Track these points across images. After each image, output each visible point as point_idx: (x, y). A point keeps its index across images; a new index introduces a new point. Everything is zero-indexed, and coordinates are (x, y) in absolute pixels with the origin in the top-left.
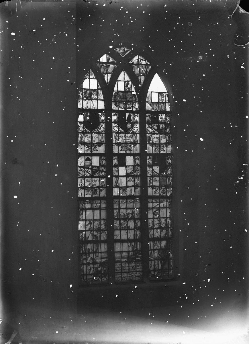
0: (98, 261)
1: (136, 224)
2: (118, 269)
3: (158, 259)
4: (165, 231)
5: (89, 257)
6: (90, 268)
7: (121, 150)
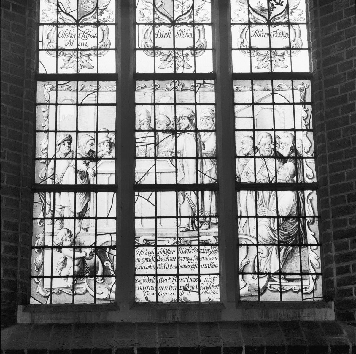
0: (87, 240)
1: (199, 144)
4: (290, 166)
6: (62, 260)
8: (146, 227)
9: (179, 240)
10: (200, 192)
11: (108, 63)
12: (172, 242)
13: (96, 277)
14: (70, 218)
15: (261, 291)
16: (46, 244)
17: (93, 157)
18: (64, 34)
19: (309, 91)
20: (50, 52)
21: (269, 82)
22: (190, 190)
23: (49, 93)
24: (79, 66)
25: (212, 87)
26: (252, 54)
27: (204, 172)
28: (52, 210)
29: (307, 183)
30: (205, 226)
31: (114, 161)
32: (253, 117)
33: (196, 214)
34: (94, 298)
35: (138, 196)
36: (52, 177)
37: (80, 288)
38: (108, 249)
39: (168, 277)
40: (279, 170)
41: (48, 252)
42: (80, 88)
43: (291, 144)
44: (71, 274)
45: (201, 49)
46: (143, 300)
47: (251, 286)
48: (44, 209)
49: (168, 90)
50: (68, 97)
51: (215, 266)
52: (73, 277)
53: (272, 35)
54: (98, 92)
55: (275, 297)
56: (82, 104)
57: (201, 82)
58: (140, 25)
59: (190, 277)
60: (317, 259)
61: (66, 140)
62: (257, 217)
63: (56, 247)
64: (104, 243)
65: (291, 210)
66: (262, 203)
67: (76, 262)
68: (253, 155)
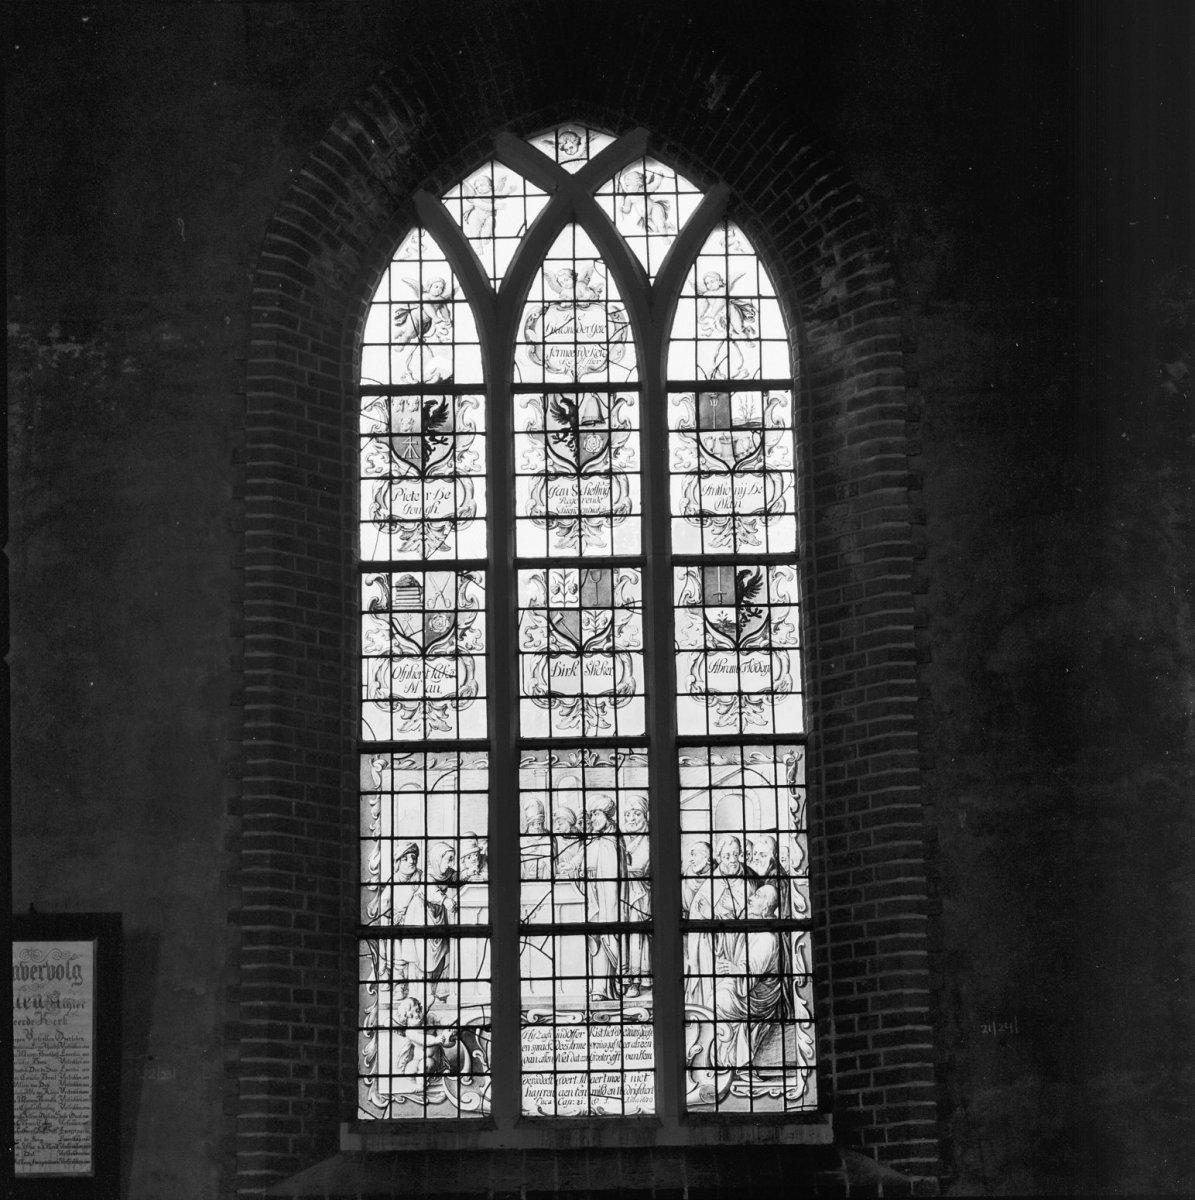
0: (446, 1016)
1: (623, 857)
2: (540, 1054)
4: (768, 892)
6: (407, 1048)
7: (561, 546)
9: (591, 1015)
10: (623, 936)
11: (475, 723)
12: (579, 1018)
14: (417, 981)
15: (720, 1097)
16: (380, 1024)
17: (452, 881)
18: (403, 672)
19: (802, 764)
20: (380, 703)
21: (737, 749)
22: (609, 934)
24: (428, 728)
25: (644, 760)
27: (631, 904)
28: (389, 967)
29: (796, 921)
30: (632, 992)
31: (487, 885)
32: (711, 810)
33: (618, 972)
34: (456, 1110)
35: (526, 943)
36: (387, 914)
37: (435, 1093)
38: (478, 1031)
39: (573, 1075)
41: (384, 1036)
42: (430, 764)
43: (770, 855)
44: (421, 1071)
45: (626, 696)
46: (534, 1112)
47: (705, 1088)
48: (377, 967)
49: (573, 766)
51: (648, 1056)
52: (424, 1075)
53: (742, 669)
54: (458, 770)
55: (741, 1106)
56: (432, 792)
57: (626, 751)
58: (525, 656)
59: (608, 1074)
60: (810, 1045)
61: (408, 853)
62: (714, 976)
63: (397, 1029)
64: (472, 1021)
65: (770, 964)
66: (723, 952)
68: (708, 874)
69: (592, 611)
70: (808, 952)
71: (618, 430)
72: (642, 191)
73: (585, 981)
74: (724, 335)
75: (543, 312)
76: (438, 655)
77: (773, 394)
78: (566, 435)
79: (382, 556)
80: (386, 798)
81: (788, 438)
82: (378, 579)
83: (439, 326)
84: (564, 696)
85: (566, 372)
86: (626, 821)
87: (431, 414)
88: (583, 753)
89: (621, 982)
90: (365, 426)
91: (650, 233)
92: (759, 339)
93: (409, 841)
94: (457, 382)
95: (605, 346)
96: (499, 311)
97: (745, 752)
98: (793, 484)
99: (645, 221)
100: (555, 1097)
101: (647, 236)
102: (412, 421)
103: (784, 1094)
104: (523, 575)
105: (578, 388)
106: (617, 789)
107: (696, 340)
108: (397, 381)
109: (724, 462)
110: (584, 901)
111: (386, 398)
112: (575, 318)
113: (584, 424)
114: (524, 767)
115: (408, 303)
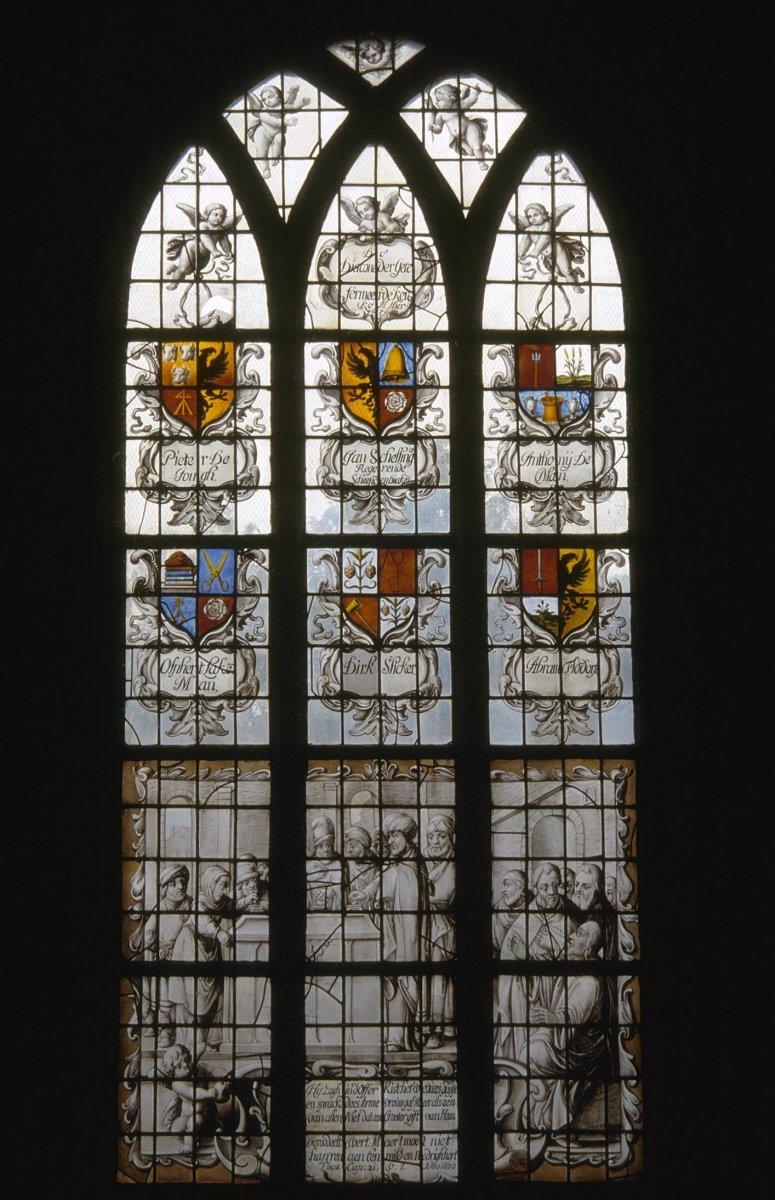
0: (219, 1067)
1: (425, 886)
2: (326, 1112)
3: (551, 1074)
4: (591, 927)
5: (172, 1043)
6: (173, 1103)
7: (355, 522)
8: (325, 1043)
9: (386, 1069)
11: (253, 724)
12: (372, 1071)
13: (235, 1135)
14: (186, 1025)
16: (143, 1074)
18: (172, 665)
19: (631, 781)
20: (146, 702)
21: (558, 763)
23: (145, 784)
24: (201, 731)
26: (527, 706)
29: (623, 962)
30: (432, 1043)
32: (526, 833)
33: (417, 1019)
35: (311, 984)
36: (153, 947)
37: (206, 1155)
38: (255, 1085)
39: (364, 1137)
40: (571, 936)
41: (147, 1090)
42: (202, 773)
43: (595, 887)
44: (191, 1129)
45: (430, 698)
46: (319, 1177)
47: (516, 1154)
49: (369, 778)
50: (180, 793)
53: (565, 669)
54: (236, 781)
56: (206, 807)
57: (430, 762)
58: (314, 649)
59: (405, 1136)
60: (636, 1105)
61: (178, 876)
62: (528, 1025)
64: (249, 1073)
66: (539, 999)
67: (198, 1106)
68: (523, 907)
69: (392, 599)
70: (636, 999)
71: (425, 387)
72: (455, 107)
73: (380, 1029)
74: (547, 278)
75: (339, 246)
76: (214, 647)
77: (604, 348)
78: (364, 392)
79: (150, 529)
80: (152, 813)
81: (621, 401)
82: (145, 557)
83: (218, 261)
84: (358, 697)
85: (365, 318)
86: (429, 844)
87: (208, 364)
88: (380, 764)
89: (420, 1031)
90: (131, 376)
91: (463, 157)
92: (589, 284)
93: (178, 863)
94: (240, 325)
95: (410, 288)
96: (288, 241)
97: (567, 767)
98: (626, 454)
99: (458, 142)
100: (343, 1160)
101: (461, 160)
102: (186, 373)
103: (605, 1162)
104: (314, 554)
105: (378, 336)
106: (418, 807)
107: (516, 282)
108: (169, 324)
109: (546, 427)
110: (379, 936)
111: (156, 344)
112: (376, 254)
113: (386, 378)
114: (311, 780)
115: (184, 233)
